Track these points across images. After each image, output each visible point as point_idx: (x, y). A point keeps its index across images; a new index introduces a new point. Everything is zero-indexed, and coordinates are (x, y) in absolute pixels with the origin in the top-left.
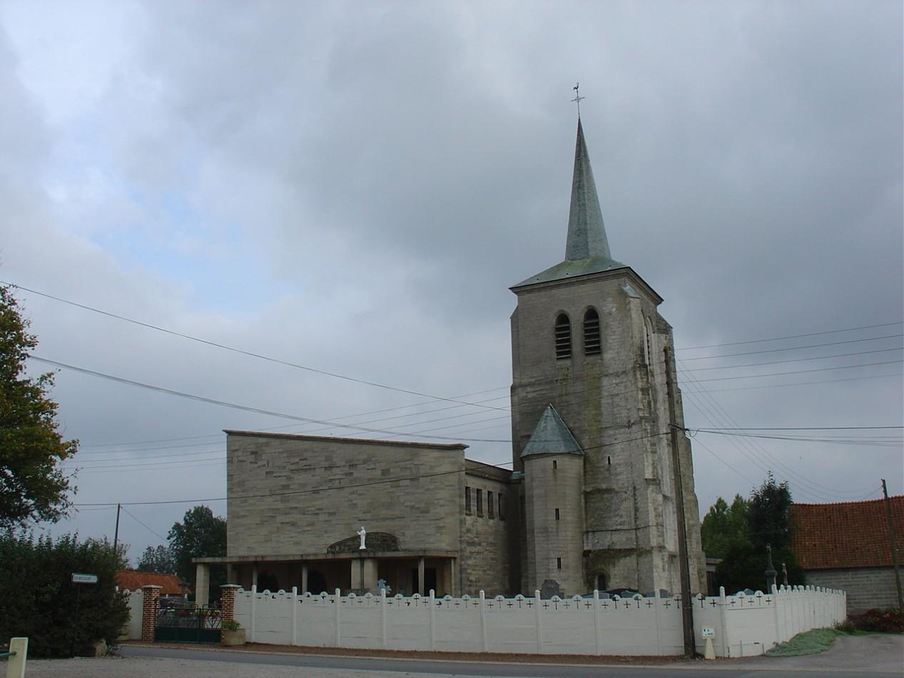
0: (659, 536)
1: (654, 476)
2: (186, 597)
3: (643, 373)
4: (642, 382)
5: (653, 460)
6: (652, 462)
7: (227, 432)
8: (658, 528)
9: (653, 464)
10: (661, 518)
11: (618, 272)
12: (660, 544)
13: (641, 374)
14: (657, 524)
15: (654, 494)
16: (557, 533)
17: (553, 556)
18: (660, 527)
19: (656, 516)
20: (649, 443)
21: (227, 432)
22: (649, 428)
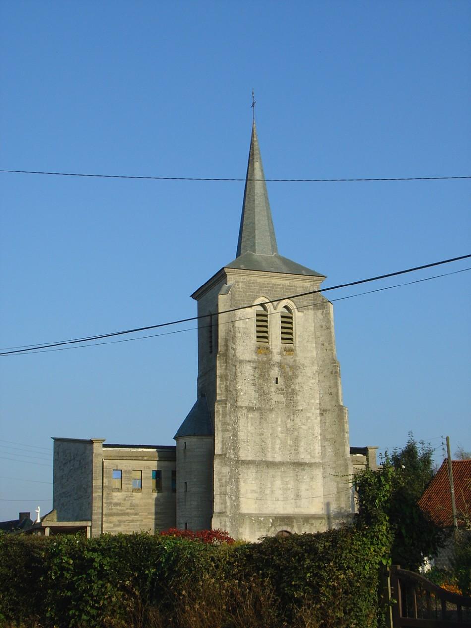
0: (222, 503)
1: (223, 451)
2: (30, 573)
3: (222, 361)
4: (221, 369)
5: (223, 438)
6: (221, 440)
7: (53, 438)
8: (221, 497)
9: (223, 441)
10: (224, 488)
11: (130, 458)
12: (222, 510)
13: (220, 363)
14: (221, 492)
15: (219, 467)
16: (186, 501)
17: (182, 522)
18: (222, 495)
19: (220, 486)
20: (220, 423)
21: (53, 438)
22: (221, 410)
